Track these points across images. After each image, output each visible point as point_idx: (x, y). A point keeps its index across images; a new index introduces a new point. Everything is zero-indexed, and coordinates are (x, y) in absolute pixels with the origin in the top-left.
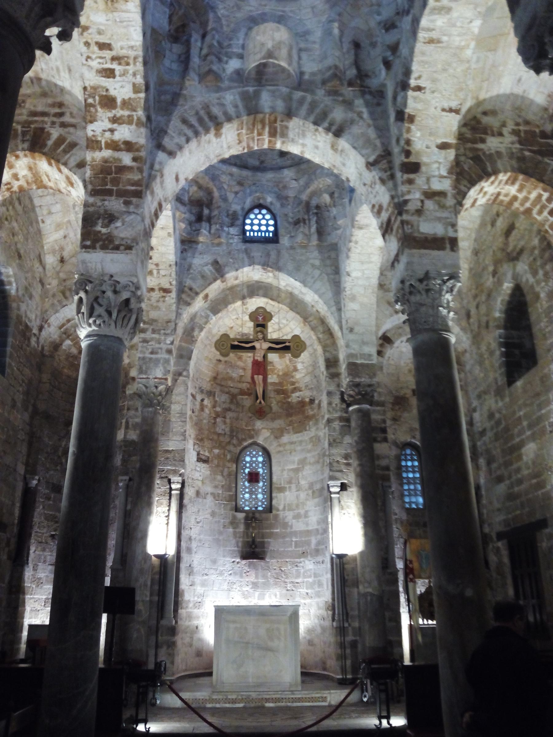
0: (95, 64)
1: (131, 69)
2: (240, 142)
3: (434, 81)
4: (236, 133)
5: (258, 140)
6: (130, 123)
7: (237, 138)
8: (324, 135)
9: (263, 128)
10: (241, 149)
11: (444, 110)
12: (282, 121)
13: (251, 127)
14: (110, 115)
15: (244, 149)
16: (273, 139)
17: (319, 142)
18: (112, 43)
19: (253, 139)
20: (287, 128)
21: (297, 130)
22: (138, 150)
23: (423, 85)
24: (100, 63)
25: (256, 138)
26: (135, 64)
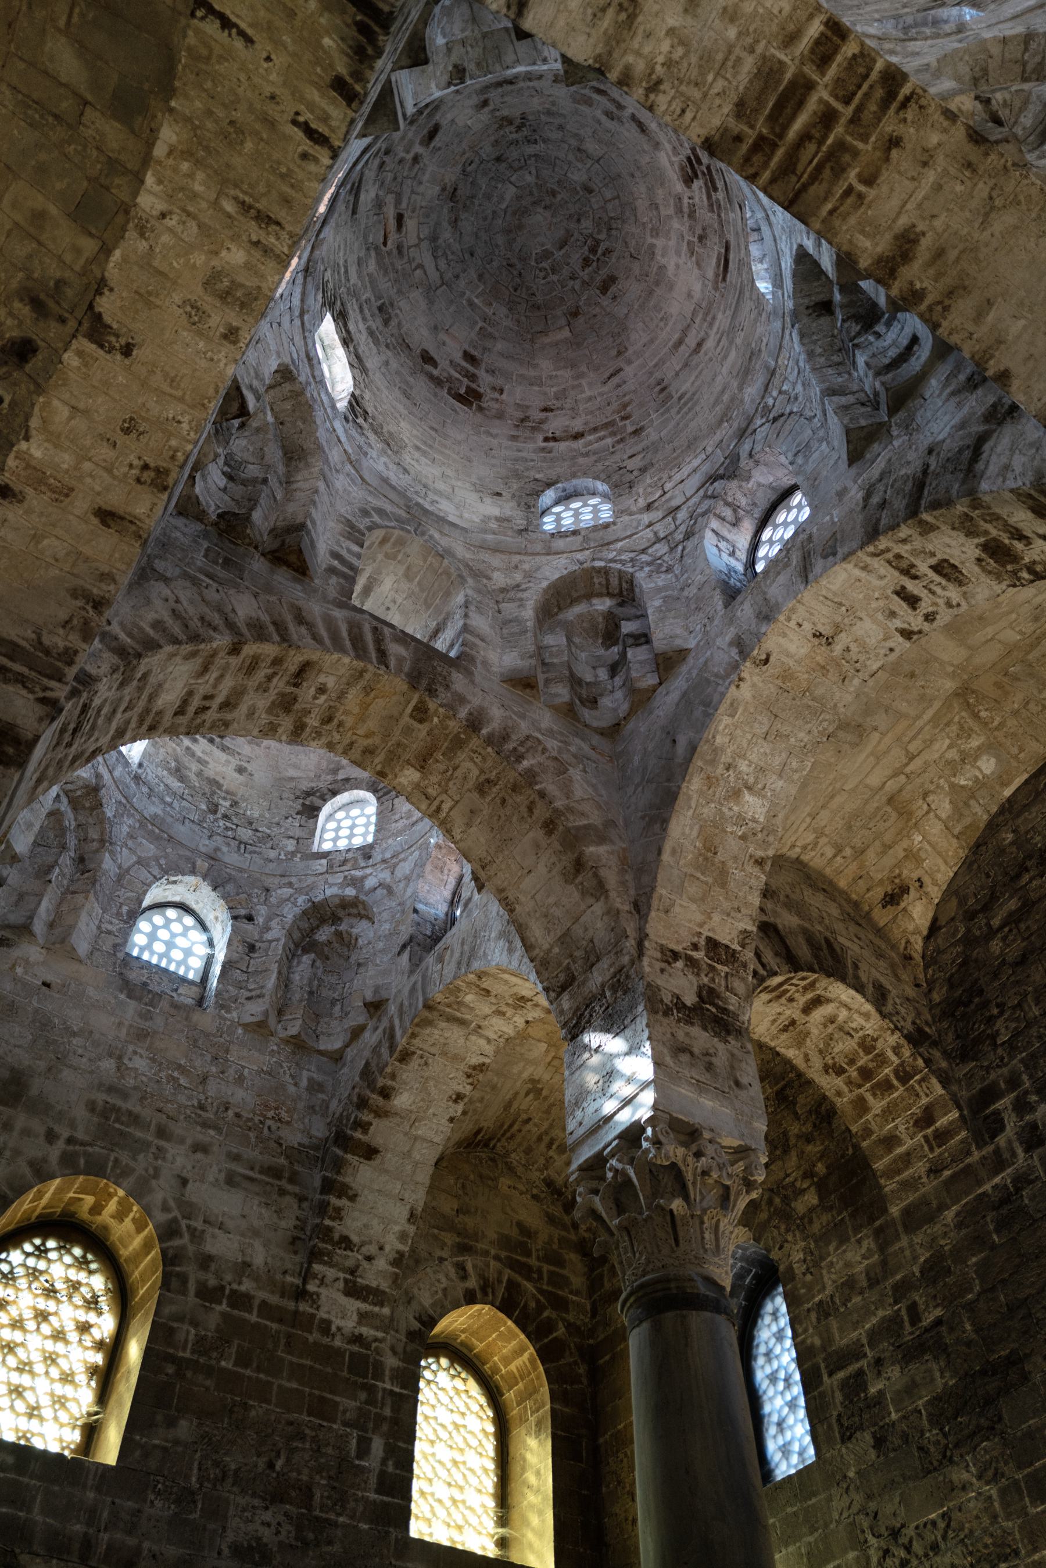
0: (953, 593)
1: (903, 550)
2: (894, 142)
3: (271, 124)
4: (871, 193)
5: (847, 102)
6: (998, 518)
7: (885, 175)
8: (640, 67)
9: (805, 137)
10: (910, 114)
11: (249, 40)
12: (738, 139)
13: (827, 173)
14: (1019, 546)
15: (904, 106)
16: (810, 71)
17: (671, 32)
18: (889, 592)
19: (855, 120)
20: (741, 109)
21: (720, 85)
22: (1030, 496)
23: (299, 134)
24: (944, 588)
25: (848, 112)
26: (888, 550)
